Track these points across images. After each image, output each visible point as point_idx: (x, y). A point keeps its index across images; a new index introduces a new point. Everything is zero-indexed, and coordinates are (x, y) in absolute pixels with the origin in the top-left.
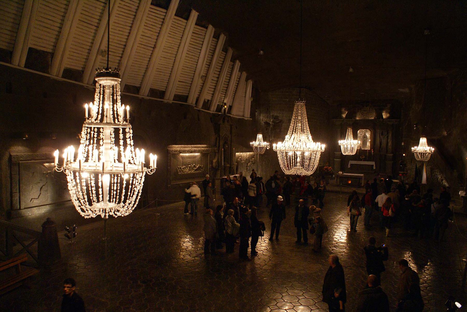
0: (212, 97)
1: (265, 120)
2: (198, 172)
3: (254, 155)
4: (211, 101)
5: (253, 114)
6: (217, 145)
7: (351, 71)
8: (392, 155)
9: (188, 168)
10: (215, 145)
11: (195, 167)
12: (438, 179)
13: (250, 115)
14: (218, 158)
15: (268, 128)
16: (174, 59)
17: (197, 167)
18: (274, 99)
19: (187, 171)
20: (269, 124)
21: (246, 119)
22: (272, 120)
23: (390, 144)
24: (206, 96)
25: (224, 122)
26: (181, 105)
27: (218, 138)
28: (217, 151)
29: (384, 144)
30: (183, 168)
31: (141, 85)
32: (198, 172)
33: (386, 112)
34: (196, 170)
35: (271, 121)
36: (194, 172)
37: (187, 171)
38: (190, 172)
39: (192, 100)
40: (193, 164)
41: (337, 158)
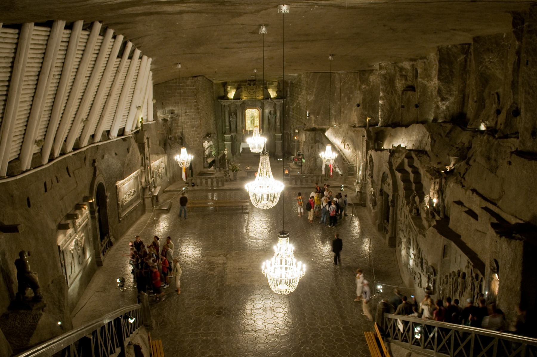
8: (281, 135)
10: (142, 165)
11: (131, 192)
15: (165, 124)
16: (118, 98)
17: (133, 191)
18: (167, 91)
20: (167, 120)
21: (150, 123)
23: (278, 124)
34: (133, 195)
37: (128, 199)
41: (227, 141)
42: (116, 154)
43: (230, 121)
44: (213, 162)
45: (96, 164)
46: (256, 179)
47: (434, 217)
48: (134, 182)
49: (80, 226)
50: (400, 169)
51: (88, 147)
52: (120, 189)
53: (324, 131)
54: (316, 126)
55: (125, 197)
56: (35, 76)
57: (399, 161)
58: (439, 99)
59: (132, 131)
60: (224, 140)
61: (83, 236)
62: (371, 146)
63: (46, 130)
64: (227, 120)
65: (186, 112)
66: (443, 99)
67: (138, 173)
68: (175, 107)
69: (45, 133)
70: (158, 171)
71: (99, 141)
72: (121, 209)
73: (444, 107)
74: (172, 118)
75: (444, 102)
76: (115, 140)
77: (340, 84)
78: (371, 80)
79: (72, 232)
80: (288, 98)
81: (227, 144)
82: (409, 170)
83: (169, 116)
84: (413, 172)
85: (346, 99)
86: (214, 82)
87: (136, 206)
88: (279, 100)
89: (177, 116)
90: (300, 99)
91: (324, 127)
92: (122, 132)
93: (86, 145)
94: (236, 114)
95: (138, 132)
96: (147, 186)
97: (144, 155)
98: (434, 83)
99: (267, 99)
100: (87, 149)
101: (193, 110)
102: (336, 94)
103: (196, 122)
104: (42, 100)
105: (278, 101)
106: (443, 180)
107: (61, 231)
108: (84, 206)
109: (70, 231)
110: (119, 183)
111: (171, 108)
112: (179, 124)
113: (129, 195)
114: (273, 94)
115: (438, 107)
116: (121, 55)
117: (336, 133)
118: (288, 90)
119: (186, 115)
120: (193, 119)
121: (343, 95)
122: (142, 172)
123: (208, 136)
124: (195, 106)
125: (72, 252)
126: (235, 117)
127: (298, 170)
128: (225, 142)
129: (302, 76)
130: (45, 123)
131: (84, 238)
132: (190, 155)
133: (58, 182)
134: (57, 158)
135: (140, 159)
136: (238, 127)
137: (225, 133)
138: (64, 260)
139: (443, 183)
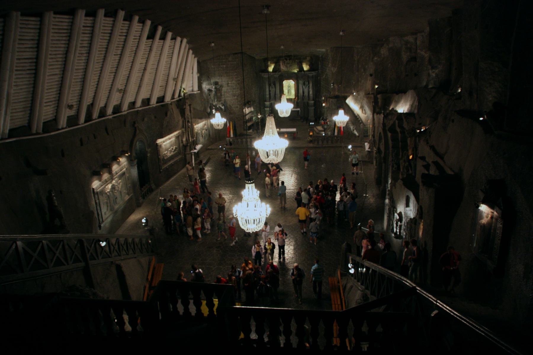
1: (208, 87)
8: (313, 102)
9: (169, 152)
10: (183, 127)
11: (173, 149)
14: (186, 138)
15: (210, 93)
17: (174, 148)
21: (195, 93)
23: (311, 93)
26: (162, 106)
27: (184, 121)
28: (185, 131)
29: (306, 94)
33: (307, 64)
34: (174, 152)
35: (213, 88)
37: (169, 155)
41: (267, 108)
42: (155, 117)
43: (270, 91)
44: (253, 125)
45: (136, 125)
46: (263, 138)
47: (408, 171)
48: (175, 141)
49: (117, 174)
50: (392, 130)
51: (128, 111)
52: (161, 146)
53: (346, 98)
54: (339, 94)
55: (166, 152)
56: (63, 54)
57: (391, 122)
58: (430, 67)
59: (173, 98)
60: (265, 107)
61: (120, 182)
62: (377, 110)
63: (80, 97)
64: (267, 90)
65: (228, 84)
66: (433, 68)
67: (179, 133)
68: (219, 79)
69: (79, 100)
70: (202, 132)
71: (139, 106)
72: (162, 162)
73: (434, 75)
74: (216, 88)
75: (434, 70)
76: (154, 106)
77: (358, 56)
78: (382, 52)
79: (108, 178)
80: (320, 71)
81: (267, 110)
82: (398, 130)
83: (214, 87)
84: (401, 132)
85: (362, 70)
86: (256, 58)
87: (177, 160)
88: (311, 72)
89: (220, 87)
90: (327, 71)
91: (346, 94)
92: (161, 99)
93: (126, 110)
94: (275, 85)
95: (180, 100)
96: (187, 144)
97: (185, 119)
98: (426, 54)
99: (301, 71)
100: (128, 113)
101: (234, 82)
102: (354, 66)
103: (237, 91)
104: (70, 72)
105: (310, 73)
106: (417, 139)
107: (95, 177)
108: (119, 158)
109: (106, 176)
110: (159, 141)
111: (217, 80)
112: (223, 94)
113: (170, 151)
114: (306, 67)
115: (429, 75)
116: (151, 36)
117: (356, 100)
118: (320, 63)
119: (228, 86)
120: (234, 89)
121: (360, 66)
122: (183, 132)
123: (247, 103)
124: (236, 78)
125: (108, 194)
126: (274, 87)
127: (323, 133)
128: (266, 109)
129: (329, 51)
130: (78, 91)
131: (121, 184)
132: (223, 118)
133: (95, 138)
134: (96, 119)
135: (181, 122)
136: (276, 96)
137: (266, 101)
138: (99, 199)
139: (417, 141)
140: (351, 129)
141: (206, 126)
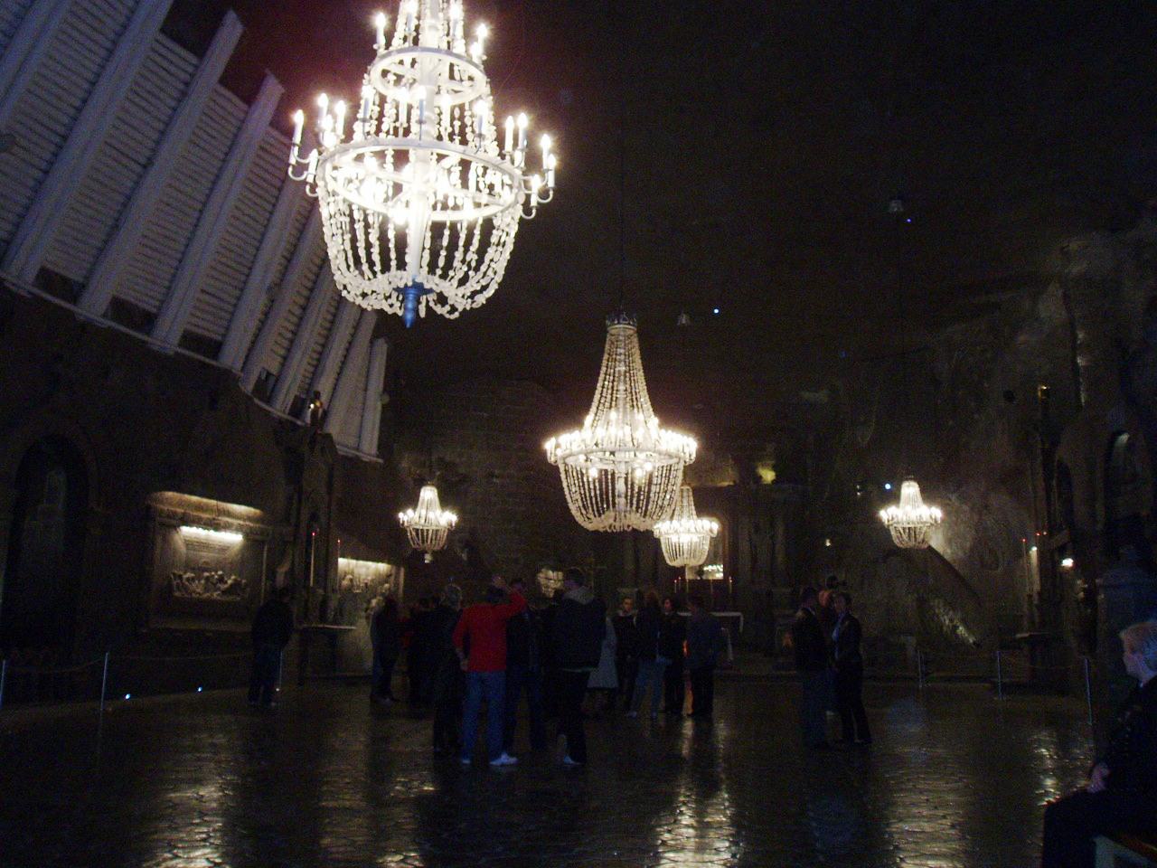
0: (283, 365)
2: (230, 598)
3: (391, 575)
4: (277, 380)
5: (384, 446)
6: (293, 521)
7: (684, 322)
9: (203, 582)
11: (221, 580)
12: (942, 627)
13: (379, 447)
17: (230, 582)
19: (198, 590)
21: (366, 459)
22: (438, 473)
23: (780, 558)
24: (268, 361)
25: (312, 449)
26: (204, 365)
27: (296, 497)
30: (188, 579)
31: (86, 278)
32: (230, 598)
34: (224, 592)
36: (219, 598)
38: (209, 594)
39: (231, 357)
40: (216, 572)
55: (189, 575)
65: (492, 475)
113: (207, 579)
140: (945, 629)
141: (387, 585)
